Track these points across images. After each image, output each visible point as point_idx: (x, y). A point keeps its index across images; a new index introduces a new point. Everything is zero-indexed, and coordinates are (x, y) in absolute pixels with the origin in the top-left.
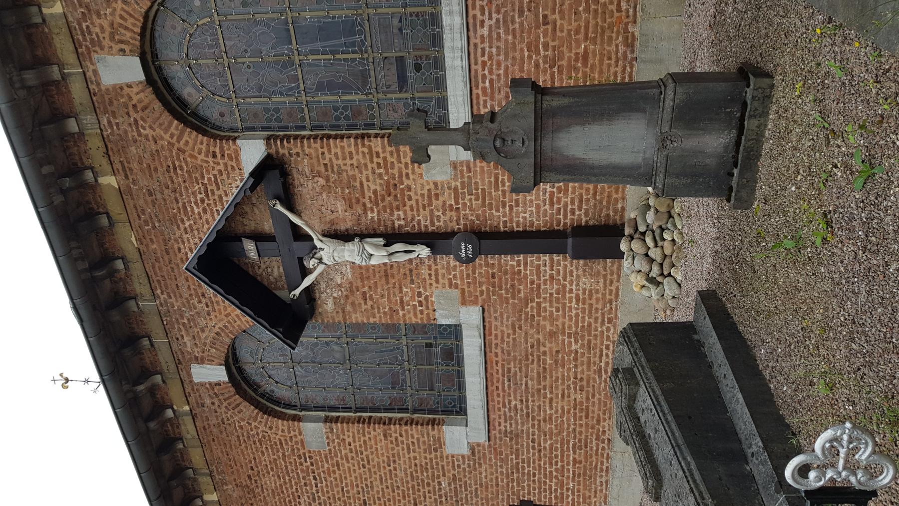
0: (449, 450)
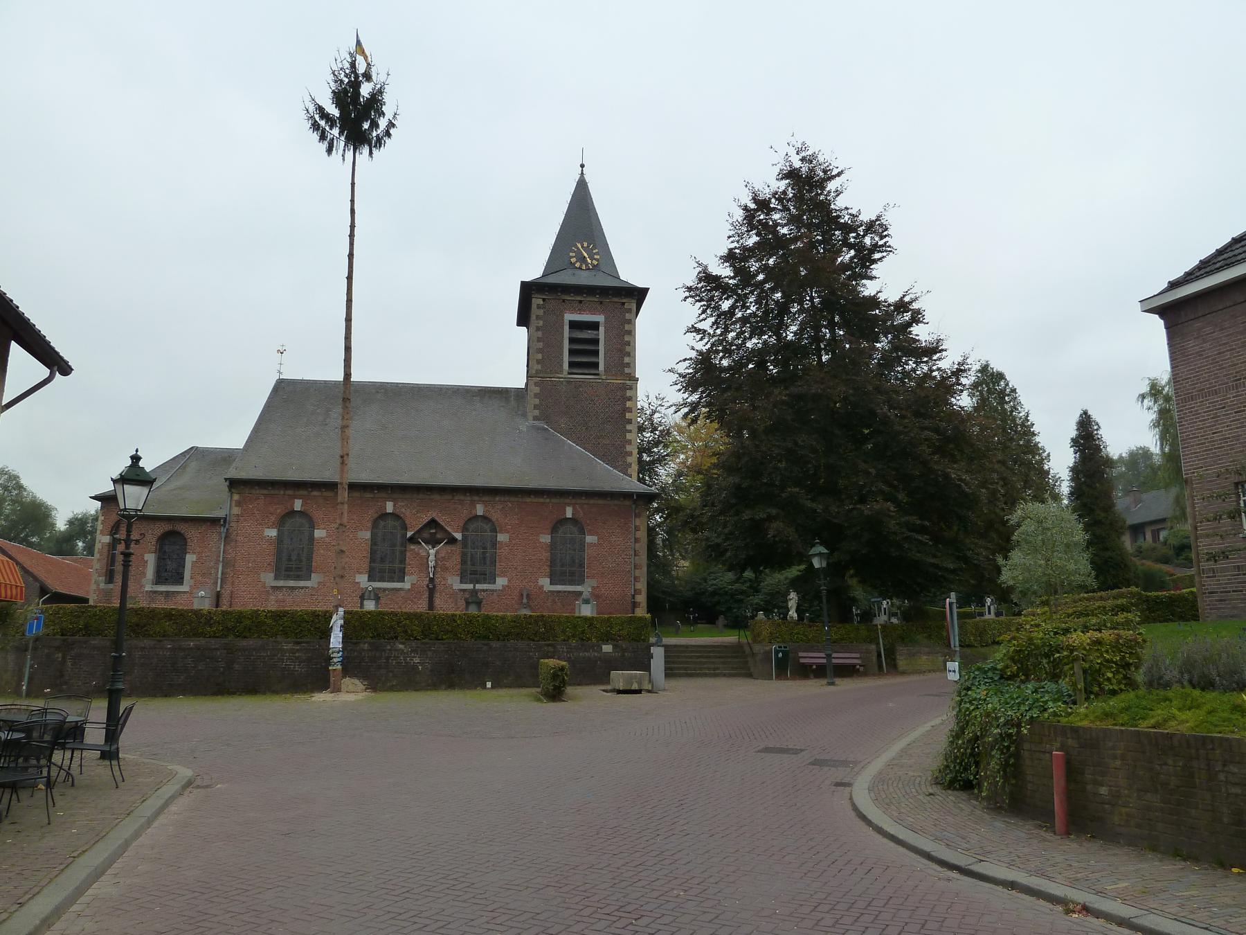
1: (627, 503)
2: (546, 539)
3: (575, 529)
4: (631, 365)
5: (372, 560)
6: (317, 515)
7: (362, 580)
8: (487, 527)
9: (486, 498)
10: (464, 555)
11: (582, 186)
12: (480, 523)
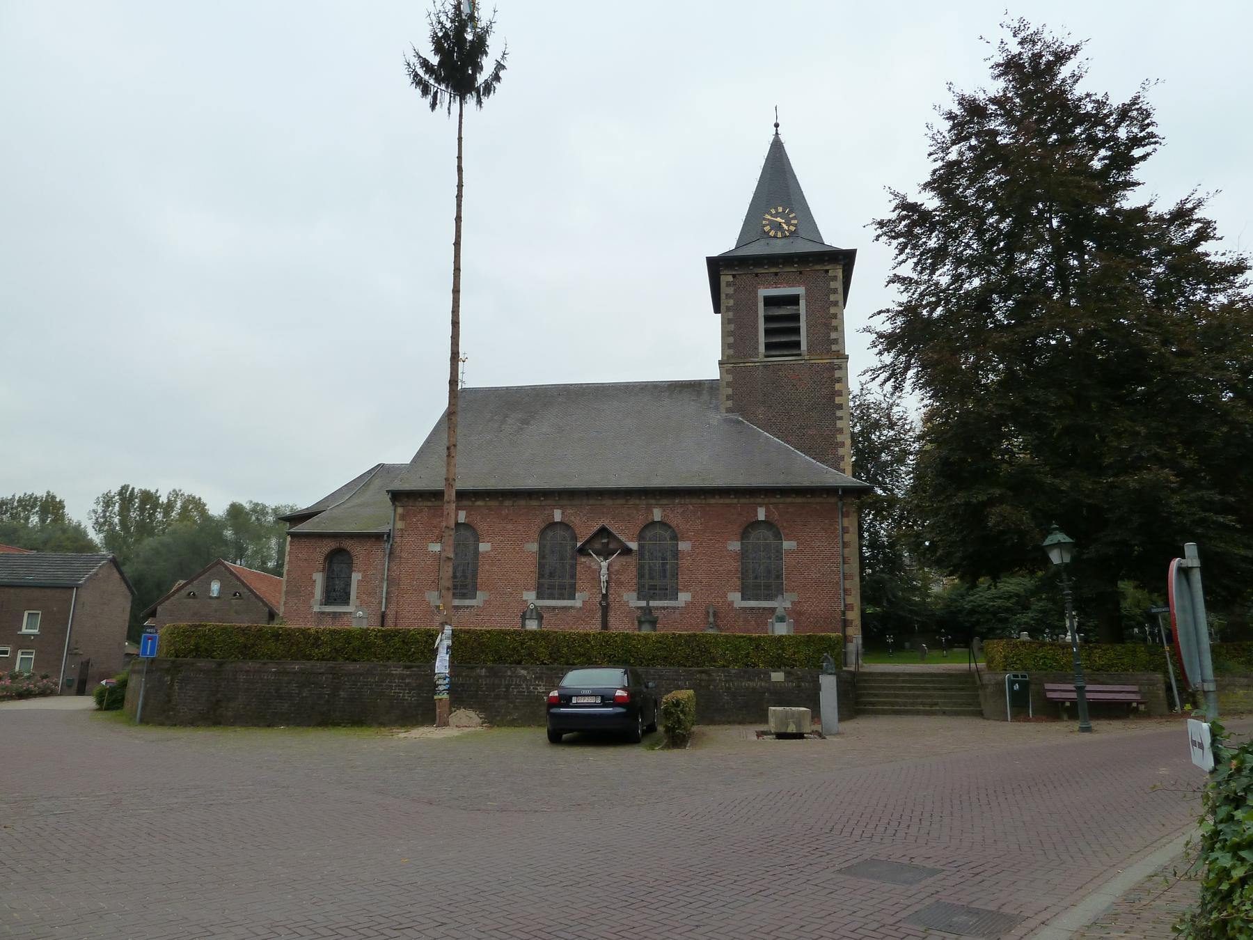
0: (525, 593)
1: (833, 500)
2: (735, 546)
3: (770, 534)
4: (840, 341)
5: (541, 576)
6: (482, 527)
7: (530, 597)
8: (667, 534)
9: (664, 501)
10: (641, 568)
11: (777, 149)
12: (658, 531)
